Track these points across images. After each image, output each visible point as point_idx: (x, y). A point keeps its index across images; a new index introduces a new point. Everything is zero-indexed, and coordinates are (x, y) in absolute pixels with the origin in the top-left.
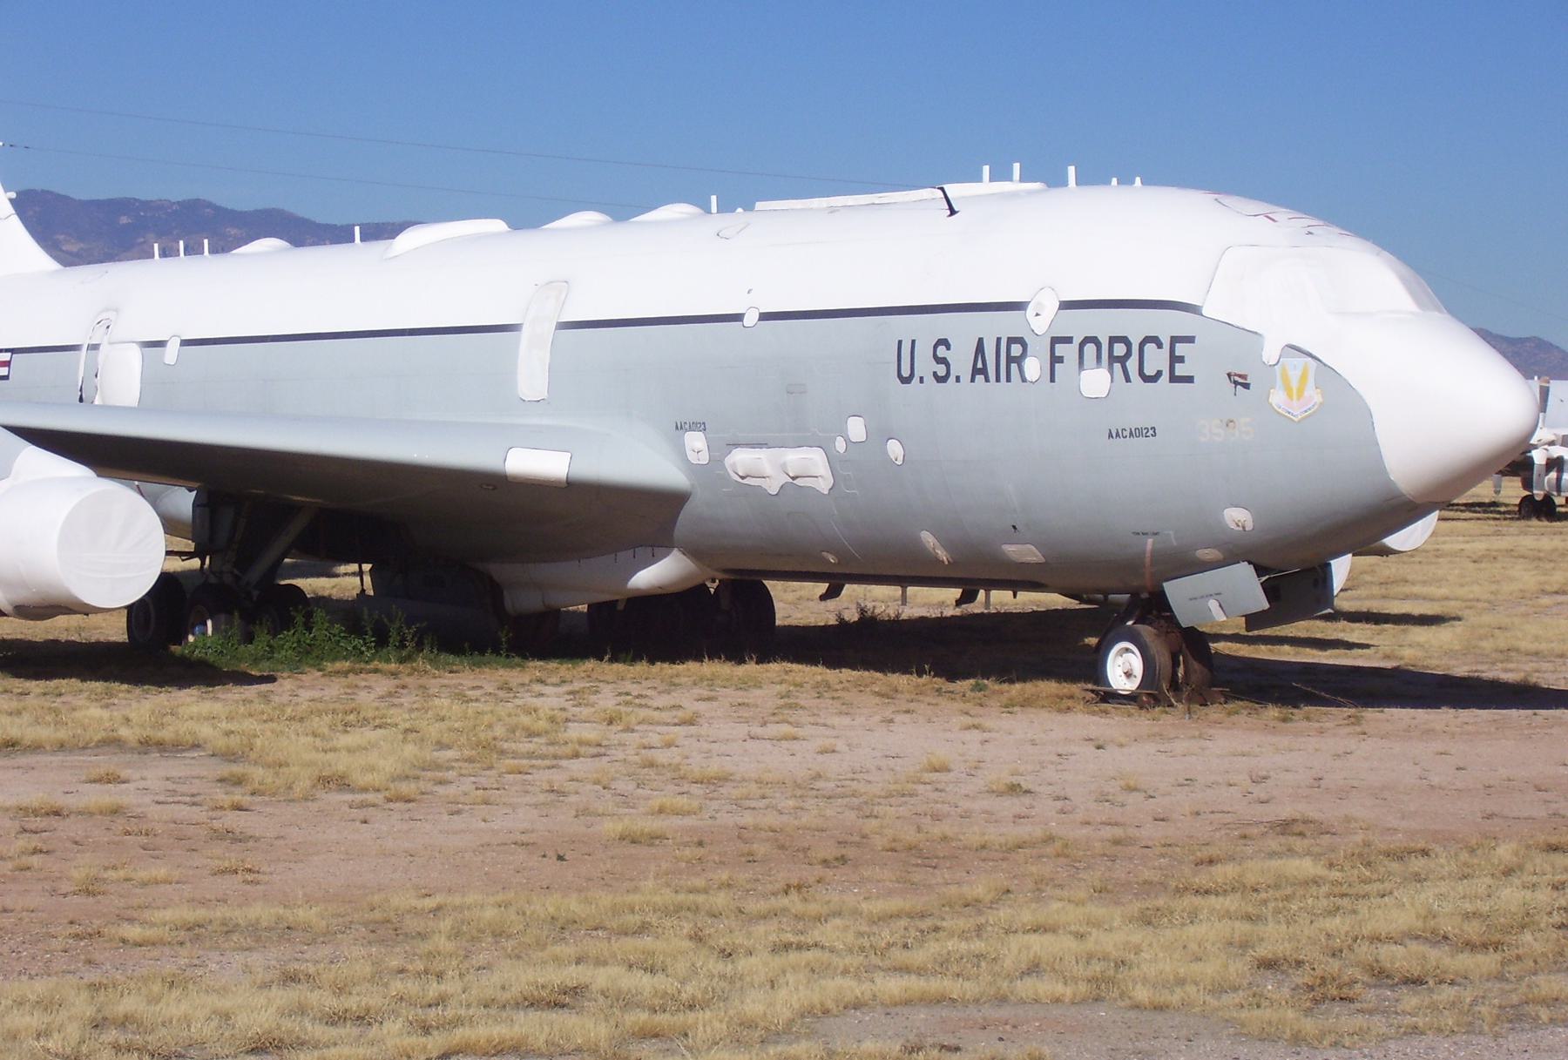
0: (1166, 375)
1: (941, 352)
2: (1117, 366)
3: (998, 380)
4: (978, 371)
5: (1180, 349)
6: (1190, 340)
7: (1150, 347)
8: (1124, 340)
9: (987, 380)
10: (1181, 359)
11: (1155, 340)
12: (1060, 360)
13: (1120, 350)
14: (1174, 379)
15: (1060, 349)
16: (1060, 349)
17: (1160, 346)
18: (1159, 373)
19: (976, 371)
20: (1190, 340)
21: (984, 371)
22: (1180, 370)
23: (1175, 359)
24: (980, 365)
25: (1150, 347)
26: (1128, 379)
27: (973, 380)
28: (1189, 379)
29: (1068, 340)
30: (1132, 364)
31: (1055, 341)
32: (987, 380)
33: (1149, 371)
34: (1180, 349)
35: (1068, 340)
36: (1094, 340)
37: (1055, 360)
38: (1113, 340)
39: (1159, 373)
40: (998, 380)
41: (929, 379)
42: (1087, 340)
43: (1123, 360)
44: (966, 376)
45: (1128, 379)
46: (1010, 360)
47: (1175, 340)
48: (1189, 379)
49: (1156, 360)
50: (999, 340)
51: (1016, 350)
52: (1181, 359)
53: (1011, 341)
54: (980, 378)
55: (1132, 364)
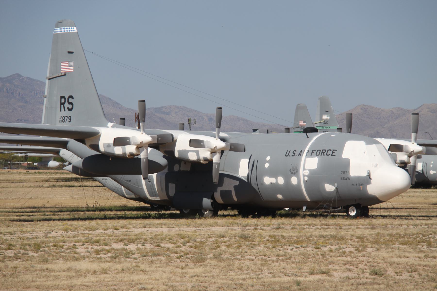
0: (331, 155)
1: (295, 152)
2: (323, 154)
5: (334, 151)
8: (325, 150)
10: (334, 153)
11: (331, 150)
12: (313, 153)
13: (324, 151)
14: (332, 155)
15: (314, 151)
18: (330, 155)
22: (333, 154)
23: (333, 152)
25: (329, 151)
26: (324, 155)
28: (335, 155)
30: (325, 153)
33: (328, 154)
34: (334, 151)
35: (316, 150)
36: (320, 150)
39: (330, 155)
41: (291, 156)
43: (324, 153)
45: (324, 155)
47: (333, 150)
48: (335, 155)
49: (330, 153)
52: (334, 153)
54: (300, 156)
55: (325, 153)
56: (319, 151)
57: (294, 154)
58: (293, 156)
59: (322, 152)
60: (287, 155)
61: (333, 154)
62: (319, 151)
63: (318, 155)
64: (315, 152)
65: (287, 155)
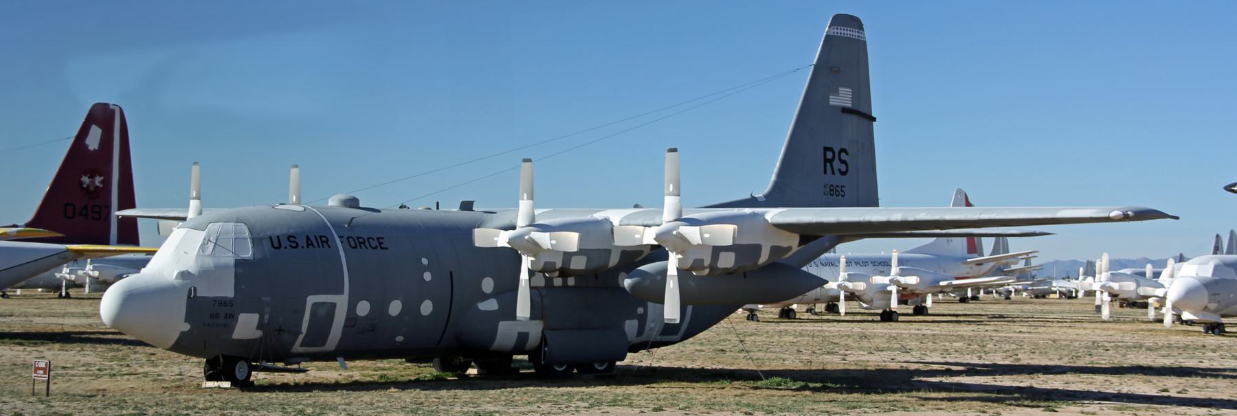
3: (319, 247)
7: (371, 240)
9: (314, 247)
10: (382, 243)
14: (382, 248)
17: (374, 240)
21: (312, 244)
23: (380, 243)
24: (310, 242)
26: (367, 248)
27: (308, 247)
30: (367, 244)
32: (314, 247)
33: (373, 246)
40: (319, 247)
43: (364, 243)
45: (367, 248)
46: (322, 242)
50: (315, 237)
54: (311, 247)
55: (367, 244)
57: (294, 245)
60: (276, 244)
65: (276, 244)
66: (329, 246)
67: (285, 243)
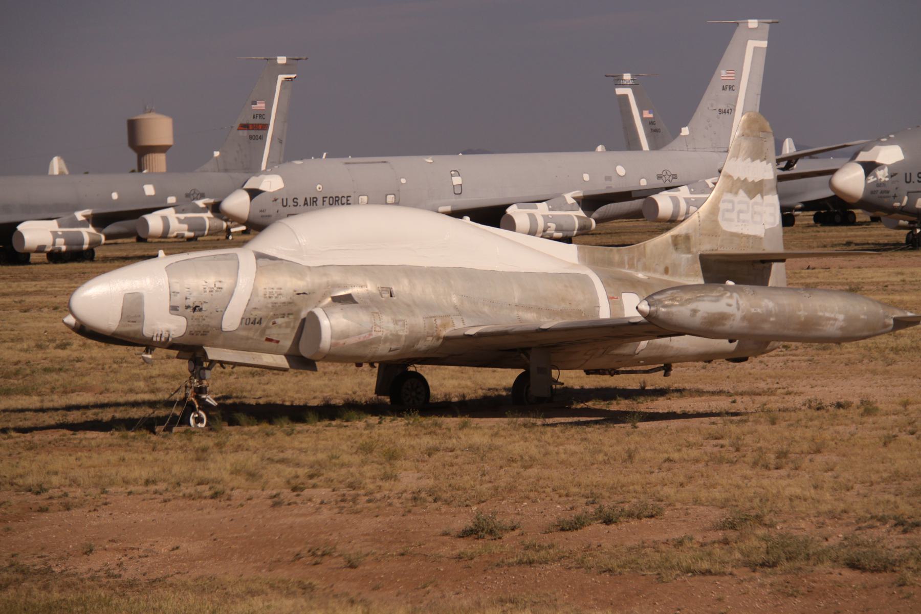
1: (295, 200)
4: (306, 204)
5: (349, 198)
6: (350, 197)
13: (337, 199)
14: (348, 204)
15: (325, 199)
16: (325, 199)
19: (305, 204)
20: (350, 197)
21: (307, 204)
22: (349, 202)
23: (348, 200)
29: (326, 197)
30: (340, 202)
31: (324, 198)
33: (343, 202)
35: (326, 197)
37: (324, 201)
38: (336, 197)
42: (330, 197)
43: (338, 201)
44: (303, 204)
46: (313, 202)
47: (348, 197)
49: (344, 200)
51: (315, 200)
53: (313, 198)
54: (306, 206)
56: (331, 199)
58: (297, 205)
59: (336, 201)
60: (285, 204)
61: (349, 202)
62: (331, 199)
63: (332, 205)
64: (327, 200)
66: (316, 205)
67: (290, 203)
